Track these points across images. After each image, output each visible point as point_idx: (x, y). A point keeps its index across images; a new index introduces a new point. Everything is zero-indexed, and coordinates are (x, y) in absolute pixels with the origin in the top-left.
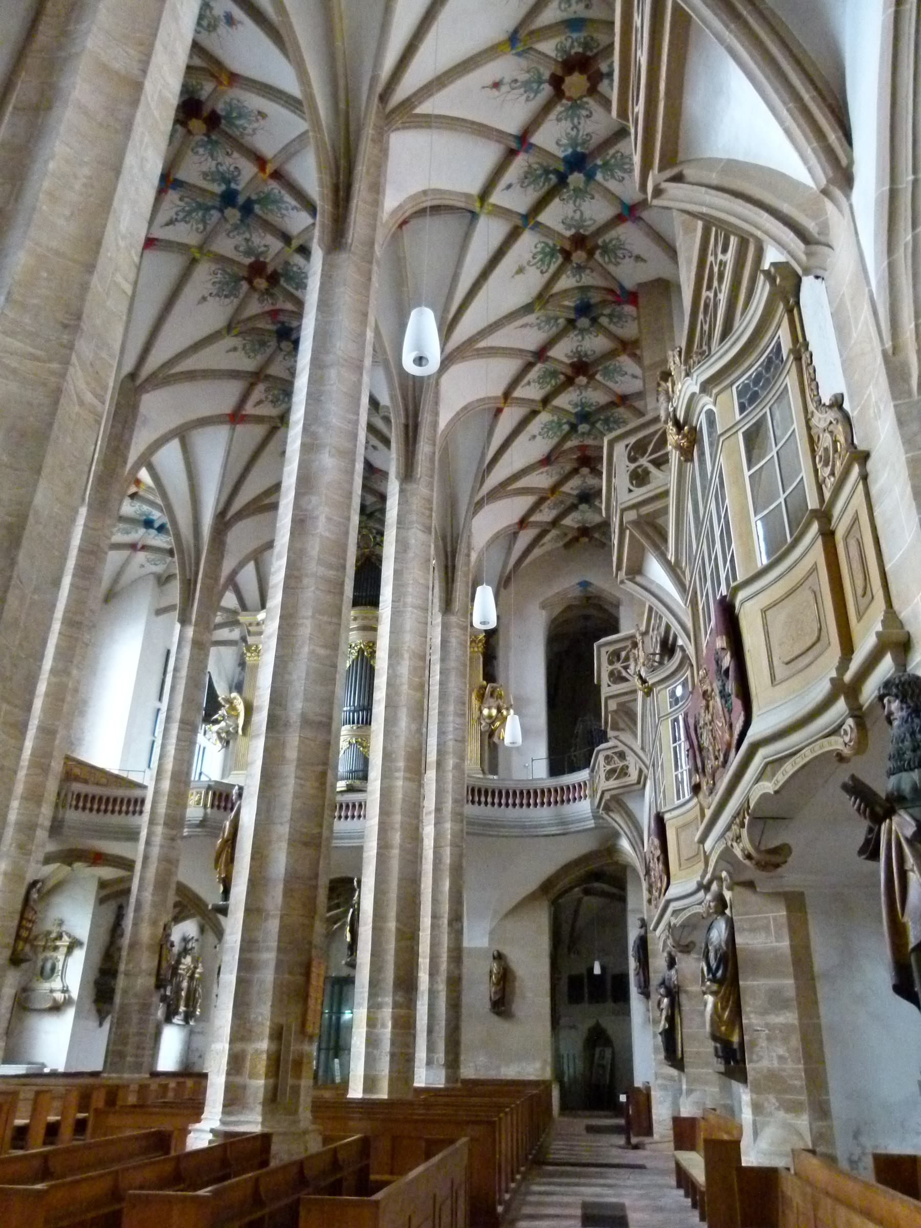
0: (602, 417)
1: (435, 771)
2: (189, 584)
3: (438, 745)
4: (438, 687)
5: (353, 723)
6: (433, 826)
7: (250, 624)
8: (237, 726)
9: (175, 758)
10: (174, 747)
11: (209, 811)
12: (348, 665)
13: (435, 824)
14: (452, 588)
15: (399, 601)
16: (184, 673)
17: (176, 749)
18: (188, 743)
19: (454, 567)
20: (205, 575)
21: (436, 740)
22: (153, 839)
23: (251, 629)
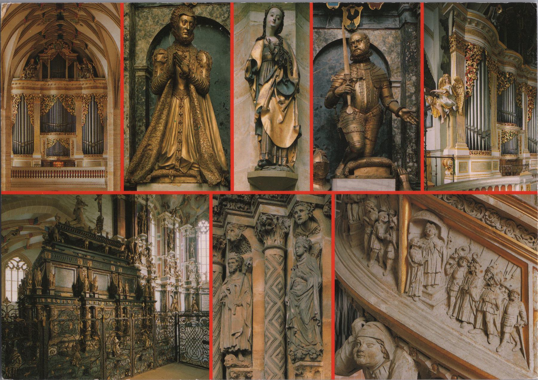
5: (57, 131)
12: (52, 105)
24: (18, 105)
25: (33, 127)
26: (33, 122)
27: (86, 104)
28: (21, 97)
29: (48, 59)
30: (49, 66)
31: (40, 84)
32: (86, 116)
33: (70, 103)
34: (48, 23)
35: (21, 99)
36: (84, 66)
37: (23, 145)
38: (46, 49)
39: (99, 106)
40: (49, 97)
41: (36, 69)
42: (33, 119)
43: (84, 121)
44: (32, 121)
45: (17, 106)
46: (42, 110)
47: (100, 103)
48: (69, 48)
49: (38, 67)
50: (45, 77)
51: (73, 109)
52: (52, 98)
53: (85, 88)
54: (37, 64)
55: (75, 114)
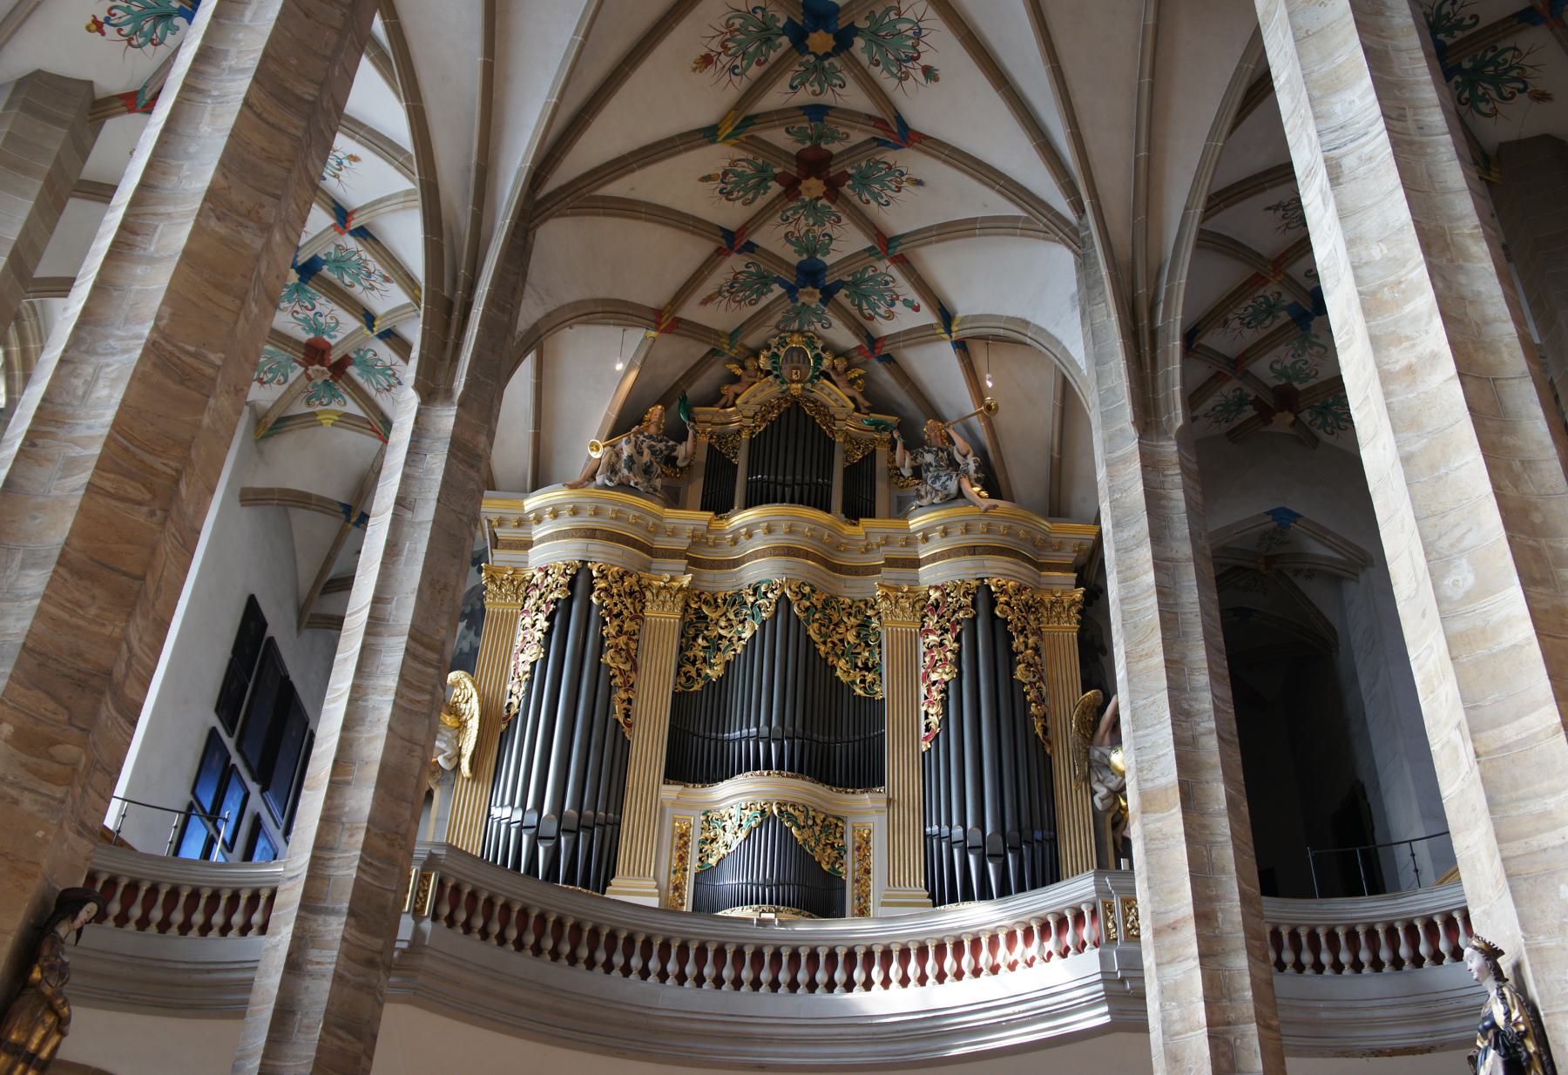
0: (1467, 65)
1: (1176, 814)
2: (449, 311)
3: (1178, 742)
4: (1154, 600)
6: (1194, 963)
7: (501, 523)
8: (459, 756)
9: (390, 728)
10: (391, 697)
11: (427, 925)
12: (747, 635)
13: (1203, 956)
14: (1154, 379)
15: (1402, 118)
16: (426, 512)
17: (395, 703)
18: (427, 697)
19: (1153, 333)
20: (492, 301)
21: (1170, 730)
22: (313, 954)
23: (501, 533)
24: (550, 618)
25: (626, 744)
26: (627, 716)
27: (947, 631)
28: (574, 578)
29: (739, 432)
30: (741, 461)
31: (691, 519)
32: (945, 691)
33: (851, 637)
34: (754, 71)
35: (571, 585)
36: (929, 458)
37: (551, 828)
38: (735, 379)
39: (1018, 643)
40: (736, 601)
41: (670, 460)
42: (630, 701)
43: (934, 720)
44: (618, 708)
45: (546, 624)
46: (684, 659)
47: (1022, 631)
48: (852, 382)
49: (682, 450)
50: (719, 504)
51: (866, 667)
52: (751, 599)
53: (933, 558)
54: (681, 437)
55: (881, 692)
